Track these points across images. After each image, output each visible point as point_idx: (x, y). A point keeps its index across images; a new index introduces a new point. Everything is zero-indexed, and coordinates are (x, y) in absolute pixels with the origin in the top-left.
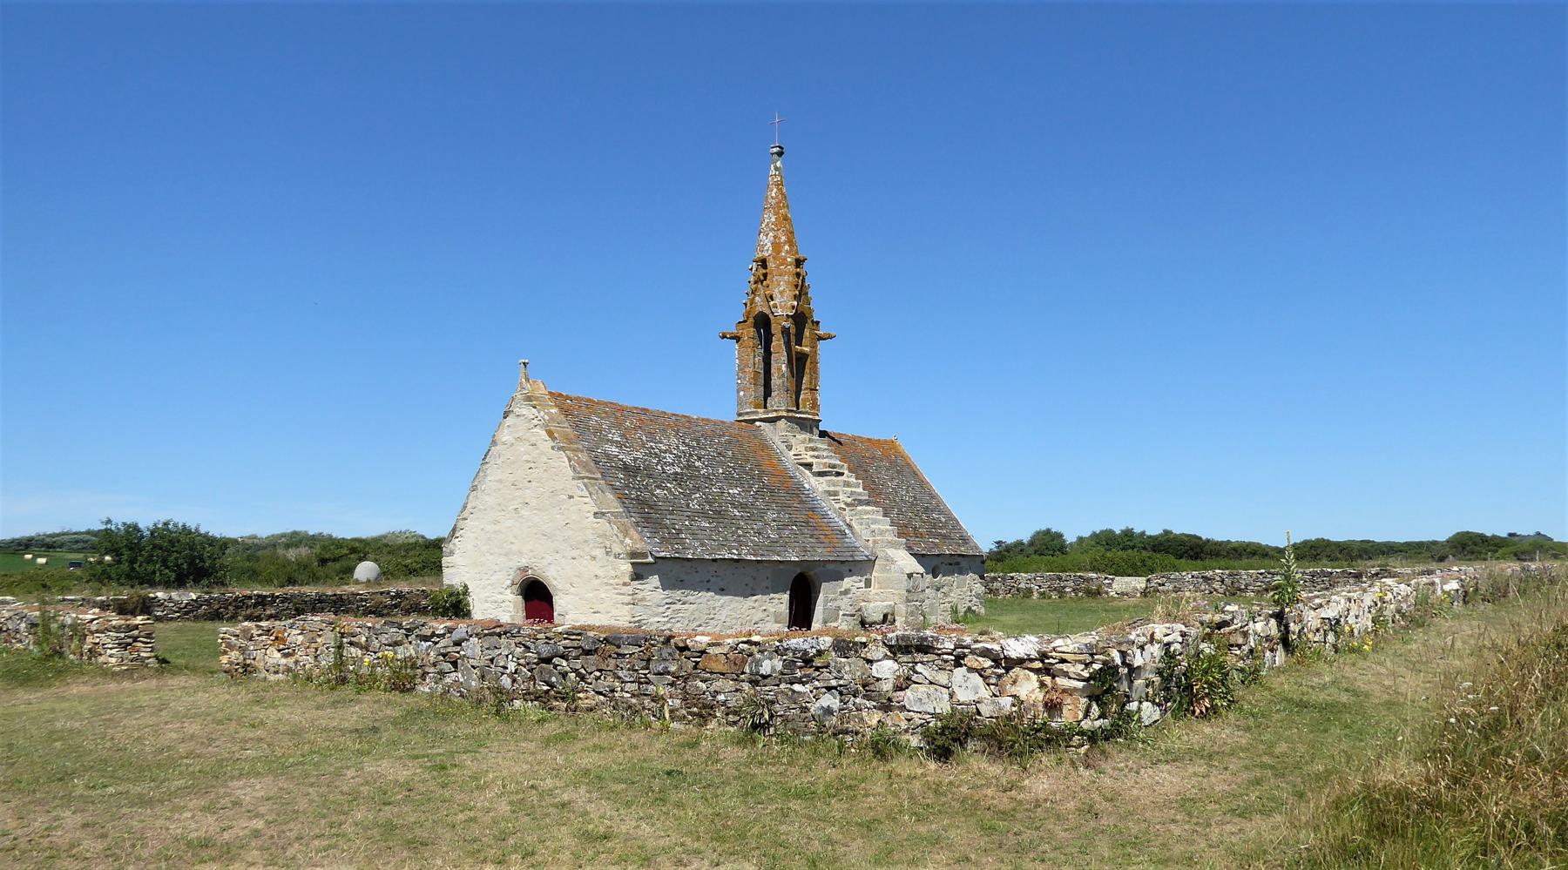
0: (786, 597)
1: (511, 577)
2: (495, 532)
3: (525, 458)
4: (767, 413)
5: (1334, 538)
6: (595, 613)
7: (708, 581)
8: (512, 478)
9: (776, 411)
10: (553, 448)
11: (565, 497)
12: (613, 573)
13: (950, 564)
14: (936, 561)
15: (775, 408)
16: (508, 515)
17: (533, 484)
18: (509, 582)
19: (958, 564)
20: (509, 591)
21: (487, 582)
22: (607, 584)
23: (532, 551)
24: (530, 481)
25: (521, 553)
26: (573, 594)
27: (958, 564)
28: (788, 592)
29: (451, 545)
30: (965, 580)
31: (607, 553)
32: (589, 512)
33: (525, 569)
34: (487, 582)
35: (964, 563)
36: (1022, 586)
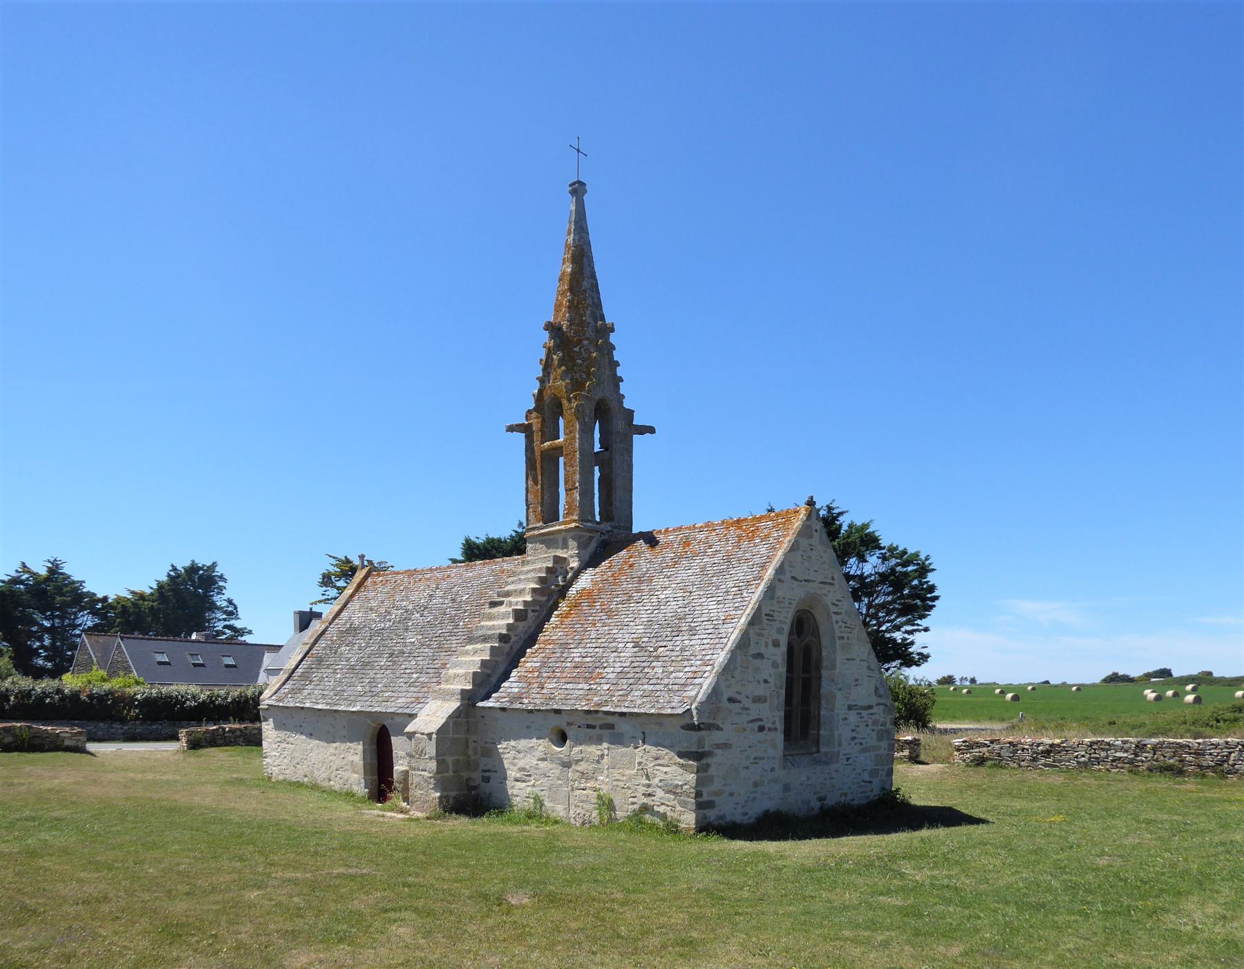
0: (360, 747)
5: (1227, 676)
7: (301, 726)
13: (593, 727)
14: (560, 722)
19: (611, 727)
27: (611, 727)
28: (361, 742)
30: (633, 756)
35: (623, 727)
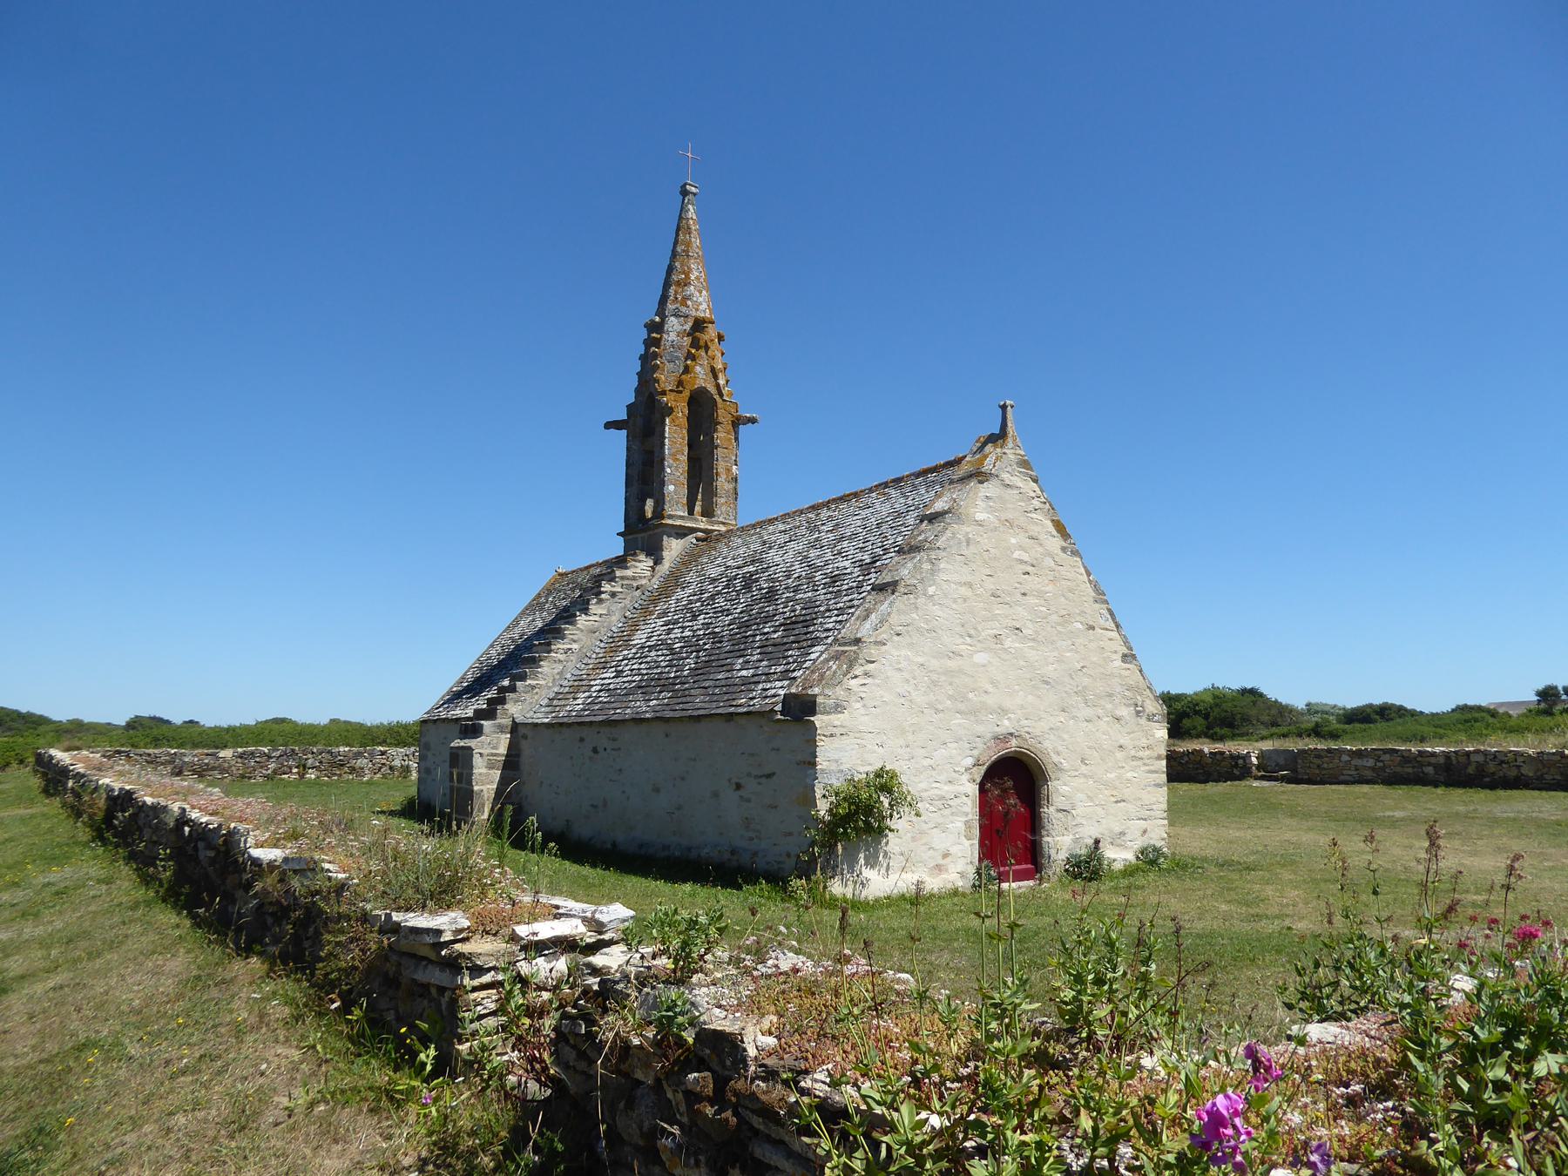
1: (976, 753)
2: (947, 672)
3: (1016, 555)
4: (713, 523)
6: (1117, 802)
8: (990, 584)
9: (723, 523)
10: (1064, 549)
11: (1081, 626)
12: (1144, 742)
15: (721, 519)
16: (979, 645)
17: (1032, 600)
18: (969, 761)
20: (966, 777)
21: (927, 762)
22: (1134, 758)
23: (1022, 707)
24: (1024, 594)
25: (1003, 711)
26: (1085, 776)
29: (839, 692)
31: (1138, 713)
32: (1116, 652)
33: (1002, 739)
34: (927, 762)
36: (397, 763)
